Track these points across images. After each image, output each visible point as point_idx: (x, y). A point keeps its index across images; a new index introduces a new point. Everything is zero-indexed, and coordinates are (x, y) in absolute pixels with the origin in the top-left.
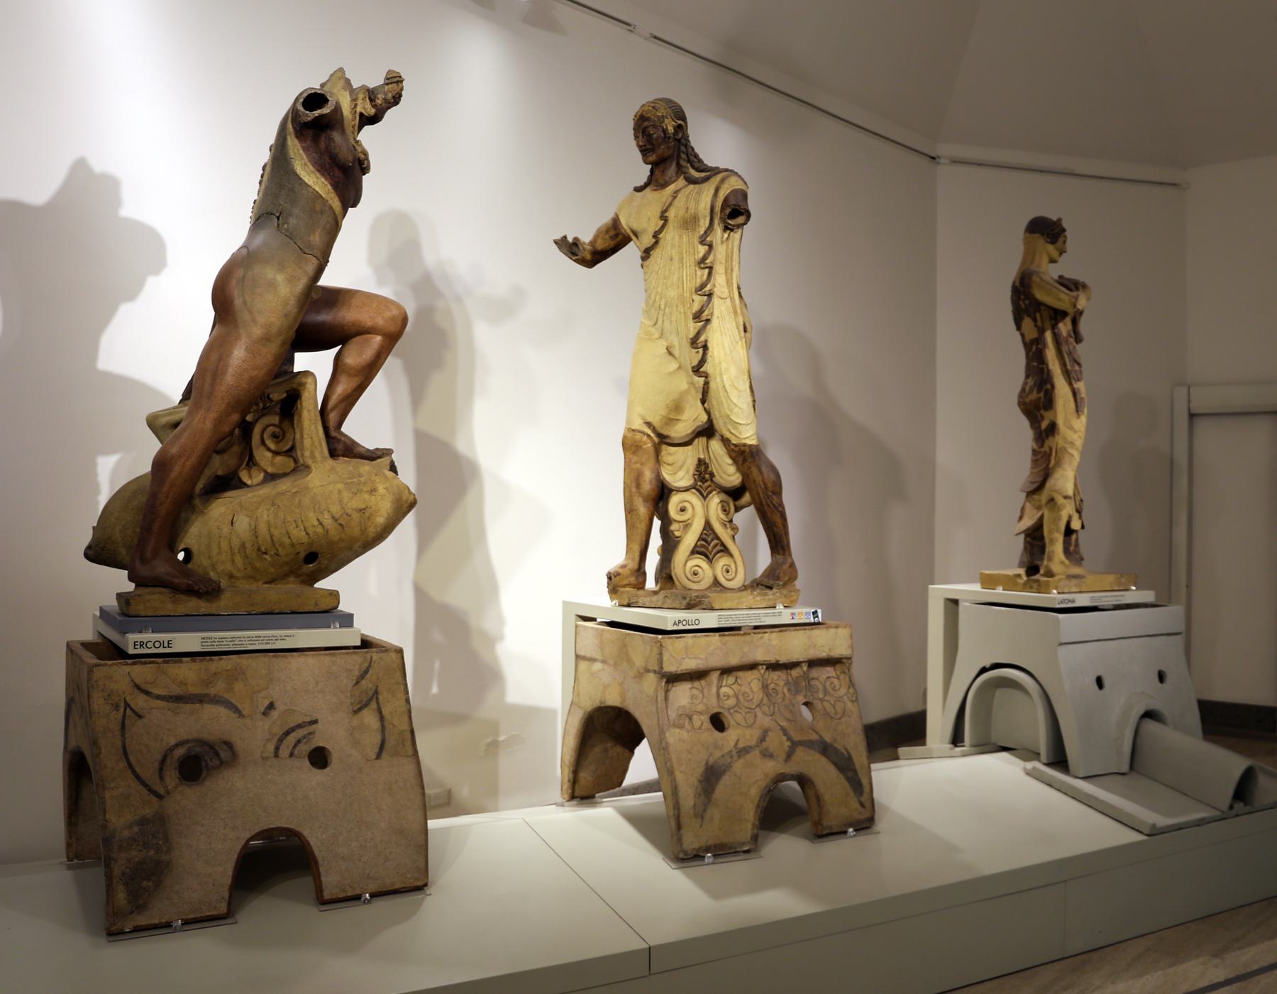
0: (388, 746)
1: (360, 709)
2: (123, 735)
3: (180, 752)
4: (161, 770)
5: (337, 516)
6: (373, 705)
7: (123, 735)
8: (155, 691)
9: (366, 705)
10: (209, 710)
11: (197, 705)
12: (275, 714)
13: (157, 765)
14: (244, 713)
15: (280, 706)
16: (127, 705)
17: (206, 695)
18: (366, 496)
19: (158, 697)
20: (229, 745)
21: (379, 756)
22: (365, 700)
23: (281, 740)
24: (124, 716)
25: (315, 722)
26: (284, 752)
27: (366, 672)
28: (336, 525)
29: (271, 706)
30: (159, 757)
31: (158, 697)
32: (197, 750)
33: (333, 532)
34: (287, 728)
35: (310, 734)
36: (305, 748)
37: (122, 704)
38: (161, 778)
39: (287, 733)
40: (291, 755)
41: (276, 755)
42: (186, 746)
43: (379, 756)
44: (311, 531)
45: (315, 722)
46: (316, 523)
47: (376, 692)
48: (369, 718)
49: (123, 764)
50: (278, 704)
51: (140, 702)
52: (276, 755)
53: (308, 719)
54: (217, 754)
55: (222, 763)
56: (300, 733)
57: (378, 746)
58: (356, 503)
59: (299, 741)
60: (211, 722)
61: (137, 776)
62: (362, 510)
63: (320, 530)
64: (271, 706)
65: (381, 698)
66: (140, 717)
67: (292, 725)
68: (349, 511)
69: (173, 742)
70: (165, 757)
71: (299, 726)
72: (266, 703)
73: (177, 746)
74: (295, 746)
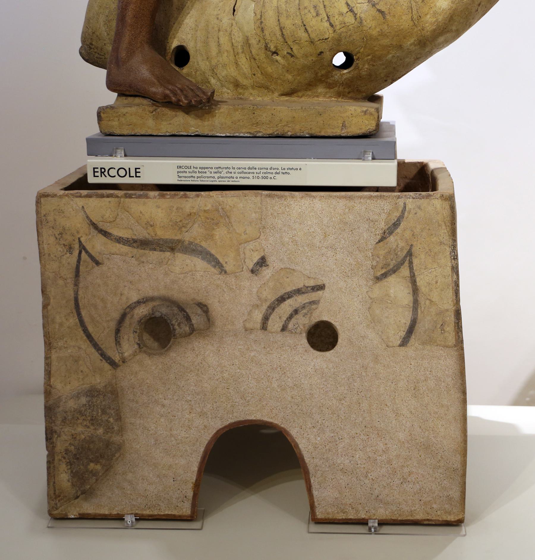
0: (420, 328)
1: (385, 275)
2: (76, 284)
3: (142, 311)
4: (118, 331)
6: (405, 271)
7: (76, 284)
8: (116, 232)
10: (182, 262)
11: (168, 254)
12: (267, 273)
13: (113, 325)
14: (227, 268)
16: (82, 248)
17: (179, 241)
19: (119, 240)
20: (204, 308)
21: (404, 342)
22: (392, 264)
23: (272, 308)
24: (79, 261)
25: (321, 287)
26: (275, 323)
27: (396, 225)
28: (373, 12)
29: (262, 262)
30: (116, 315)
31: (119, 240)
32: (164, 310)
34: (281, 292)
36: (304, 322)
37: (77, 246)
38: (118, 342)
39: (282, 299)
40: (284, 328)
41: (264, 327)
42: (151, 305)
43: (404, 342)
44: (337, 20)
45: (321, 287)
46: (345, 9)
47: (410, 254)
48: (397, 288)
49: (73, 320)
50: (270, 260)
51: (97, 245)
52: (264, 327)
53: (312, 283)
54: (188, 318)
55: (193, 330)
56: (301, 300)
59: (296, 312)
60: (183, 277)
61: (89, 337)
63: (350, 19)
64: (262, 262)
65: (415, 261)
66: (98, 263)
67: (289, 289)
69: (135, 297)
70: (124, 316)
71: (299, 292)
72: (256, 258)
73: (139, 303)
74: (291, 317)
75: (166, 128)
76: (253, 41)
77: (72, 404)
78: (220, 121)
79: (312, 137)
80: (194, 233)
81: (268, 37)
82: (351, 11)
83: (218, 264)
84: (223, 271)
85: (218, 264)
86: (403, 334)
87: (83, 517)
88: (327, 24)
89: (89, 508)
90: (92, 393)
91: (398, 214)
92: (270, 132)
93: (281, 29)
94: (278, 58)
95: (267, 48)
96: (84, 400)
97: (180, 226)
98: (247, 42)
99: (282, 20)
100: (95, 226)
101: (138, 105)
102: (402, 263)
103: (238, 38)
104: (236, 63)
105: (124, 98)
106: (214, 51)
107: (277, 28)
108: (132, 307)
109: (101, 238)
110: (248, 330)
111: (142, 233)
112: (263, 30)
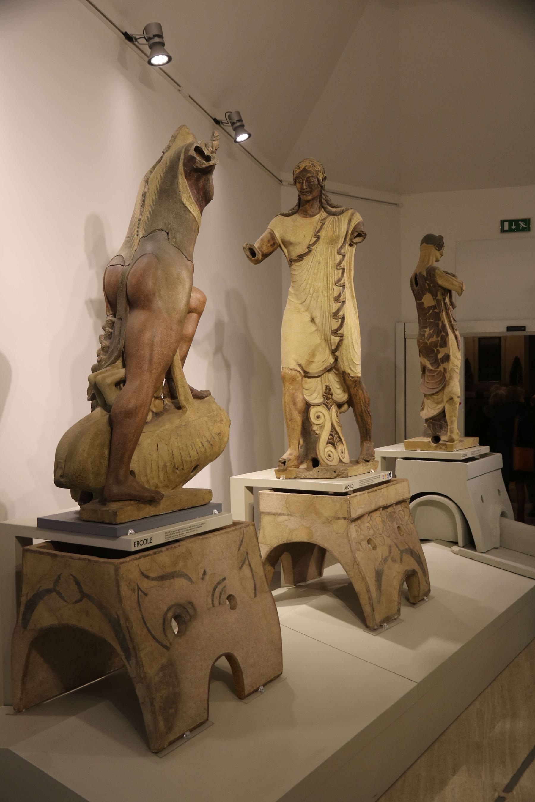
1: (242, 566)
2: (140, 610)
3: (170, 614)
4: (164, 629)
5: (209, 439)
7: (140, 610)
9: (244, 563)
11: (172, 580)
12: (207, 577)
13: (161, 626)
14: (194, 580)
15: (209, 572)
16: (139, 588)
17: (175, 572)
18: (219, 424)
19: (153, 579)
20: (191, 603)
21: (255, 596)
22: (243, 559)
23: (213, 595)
24: (138, 597)
25: (224, 579)
26: (216, 603)
29: (205, 573)
30: (161, 621)
32: (178, 611)
34: (214, 586)
35: (224, 587)
36: (224, 597)
37: (136, 588)
38: (166, 636)
39: (215, 589)
40: (220, 604)
41: (213, 606)
42: (173, 610)
43: (255, 596)
45: (224, 579)
46: (200, 445)
47: (247, 554)
48: (246, 570)
49: (145, 631)
50: (207, 571)
51: (145, 584)
52: (213, 606)
53: (221, 578)
54: (188, 612)
55: (191, 617)
56: (220, 587)
57: (253, 589)
58: (216, 430)
59: (221, 593)
60: (178, 590)
61: (154, 637)
62: (219, 434)
64: (205, 573)
65: (249, 557)
66: (146, 595)
67: (215, 583)
68: (214, 435)
69: (165, 609)
70: (164, 620)
71: (219, 583)
73: (169, 609)
74: (220, 597)
75: (142, 515)
76: (168, 464)
77: (157, 679)
78: (163, 507)
79: (193, 507)
80: (180, 566)
81: (175, 462)
82: (203, 446)
83: (190, 579)
84: (192, 582)
86: (253, 591)
87: (171, 743)
88: (196, 453)
89: (172, 737)
90: (163, 668)
91: (242, 536)
92: (179, 508)
93: (182, 457)
94: (177, 471)
95: (174, 467)
96: (161, 674)
97: (174, 564)
98: (165, 466)
99: (181, 453)
100: (143, 574)
101: (132, 505)
102: (245, 559)
103: (161, 463)
104: (159, 476)
105: (118, 502)
106: (149, 471)
107: (180, 457)
108: (166, 614)
109: (146, 580)
110: (209, 609)
111: (161, 573)
112: (174, 458)
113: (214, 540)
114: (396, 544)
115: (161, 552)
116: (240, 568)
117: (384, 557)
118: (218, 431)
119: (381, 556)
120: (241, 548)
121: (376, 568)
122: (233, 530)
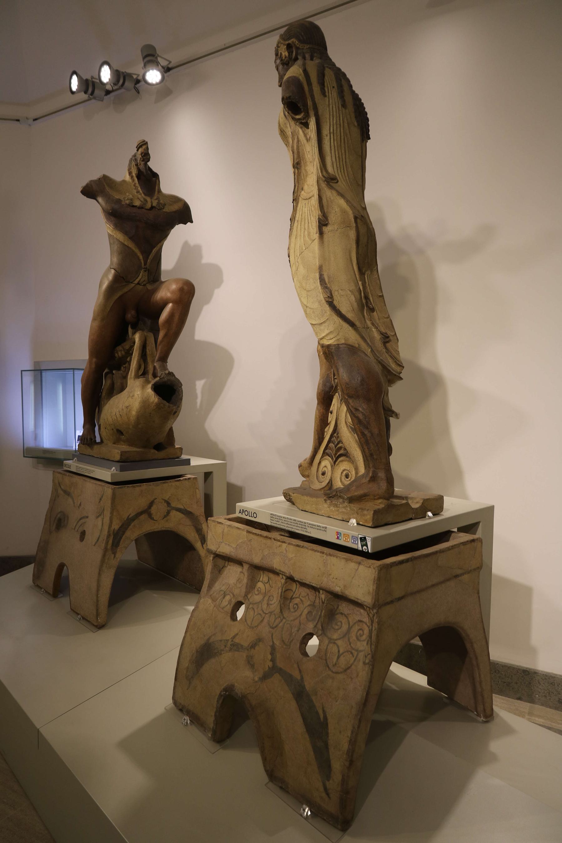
0: (99, 540)
8: (62, 487)
9: (100, 515)
10: (70, 500)
25: (87, 517)
26: (76, 530)
33: (119, 419)
35: (85, 523)
36: (81, 529)
39: (80, 519)
45: (87, 517)
47: (104, 510)
51: (60, 492)
62: (127, 407)
68: (123, 407)
83: (74, 503)
85: (74, 503)
113: (90, 485)
114: (273, 648)
115: (66, 475)
116: (97, 517)
117: (237, 640)
118: (128, 405)
119: (232, 635)
120: (101, 502)
121: (211, 641)
122: (100, 485)
